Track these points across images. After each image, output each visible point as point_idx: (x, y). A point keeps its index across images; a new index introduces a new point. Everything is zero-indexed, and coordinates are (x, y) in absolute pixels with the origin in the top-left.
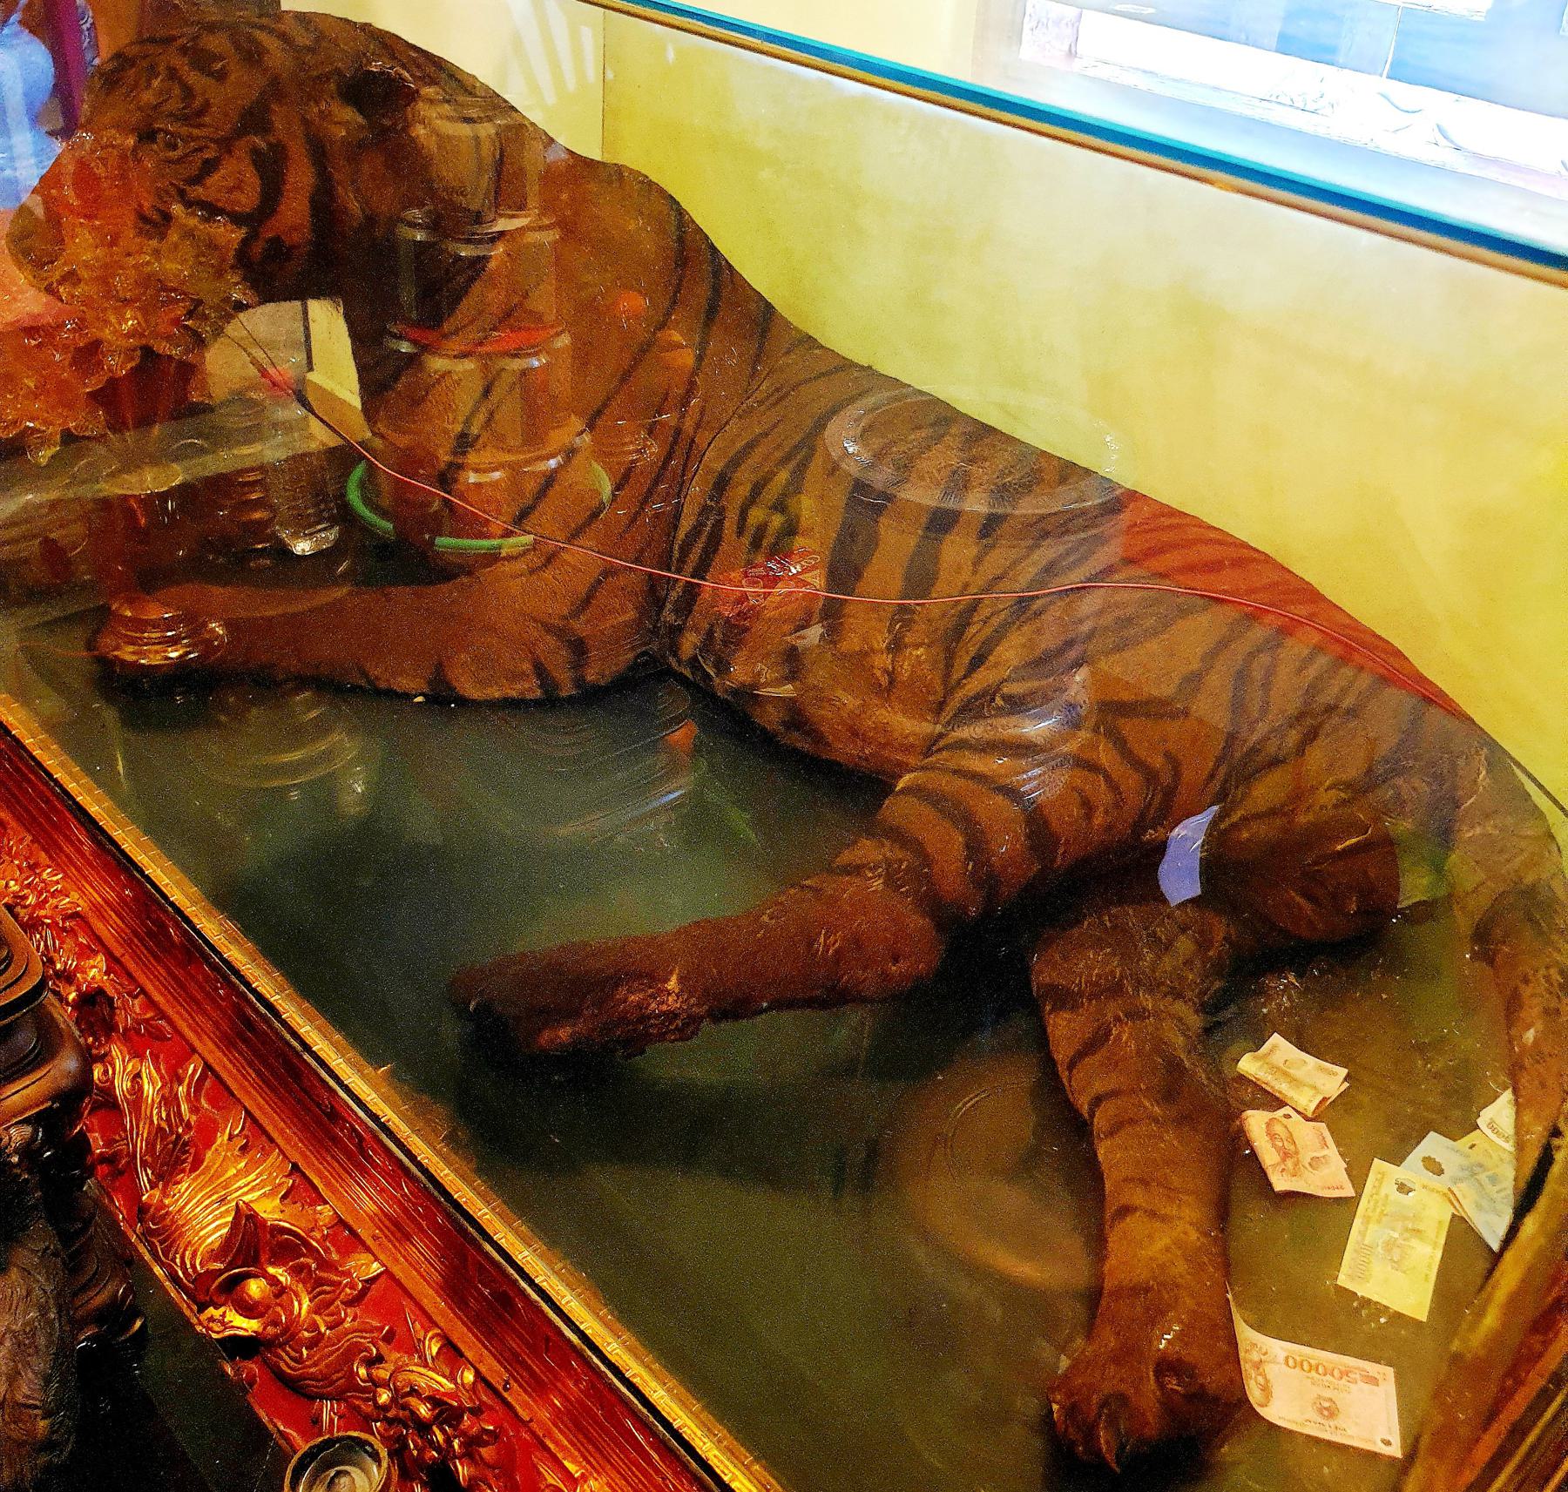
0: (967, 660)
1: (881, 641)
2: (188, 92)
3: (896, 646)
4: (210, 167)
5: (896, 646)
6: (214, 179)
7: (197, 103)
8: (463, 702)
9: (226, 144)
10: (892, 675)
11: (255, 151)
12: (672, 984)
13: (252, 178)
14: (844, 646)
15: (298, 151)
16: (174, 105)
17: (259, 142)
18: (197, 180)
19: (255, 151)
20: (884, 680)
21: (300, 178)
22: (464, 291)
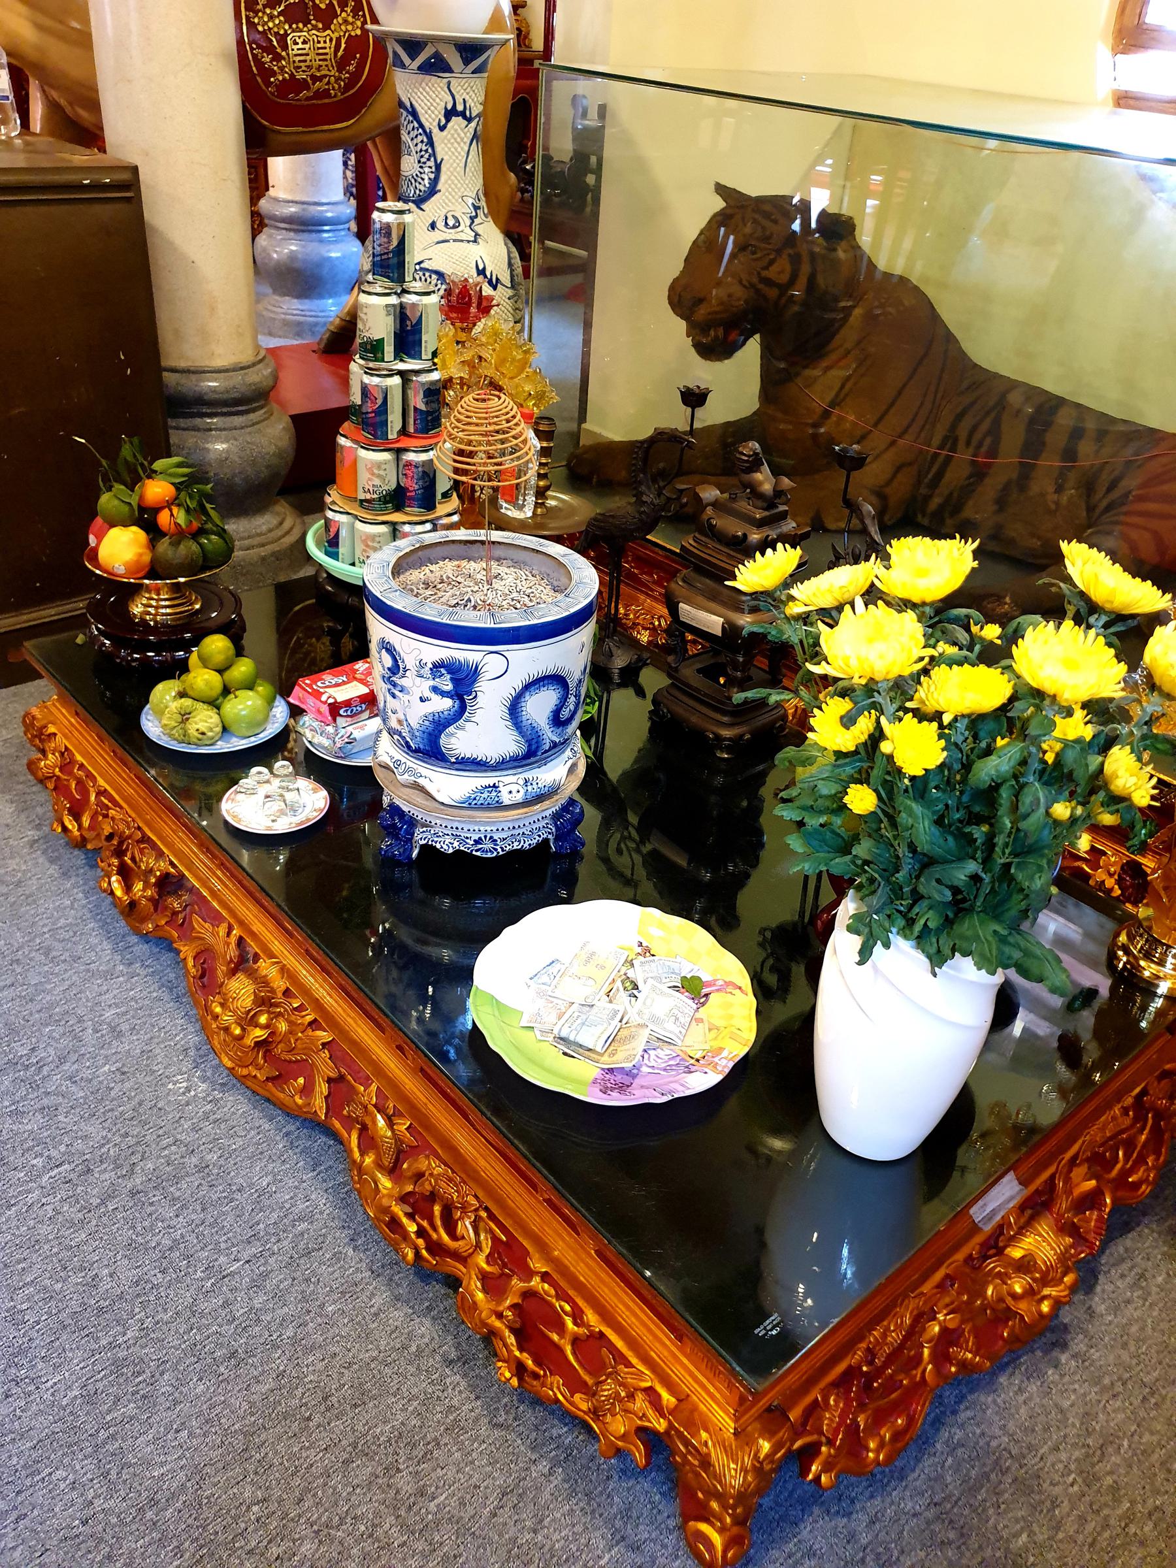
0: (1104, 489)
1: (1051, 489)
2: (763, 228)
3: (1059, 489)
4: (771, 263)
5: (1059, 489)
6: (774, 268)
7: (768, 233)
8: (826, 530)
9: (779, 252)
10: (1057, 503)
11: (790, 255)
12: (1008, 600)
13: (788, 268)
14: (1031, 493)
15: (806, 259)
16: (759, 233)
17: (791, 251)
18: (766, 268)
19: (790, 255)
20: (1053, 507)
21: (805, 269)
22: (838, 330)
